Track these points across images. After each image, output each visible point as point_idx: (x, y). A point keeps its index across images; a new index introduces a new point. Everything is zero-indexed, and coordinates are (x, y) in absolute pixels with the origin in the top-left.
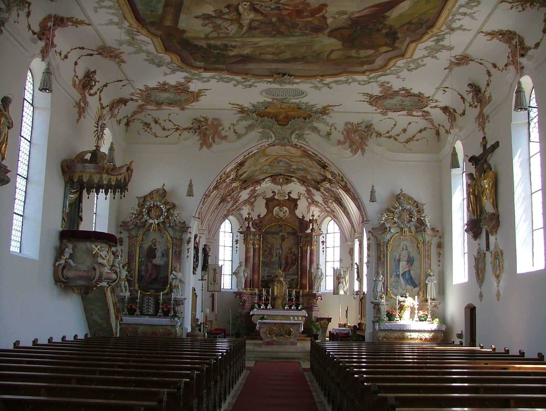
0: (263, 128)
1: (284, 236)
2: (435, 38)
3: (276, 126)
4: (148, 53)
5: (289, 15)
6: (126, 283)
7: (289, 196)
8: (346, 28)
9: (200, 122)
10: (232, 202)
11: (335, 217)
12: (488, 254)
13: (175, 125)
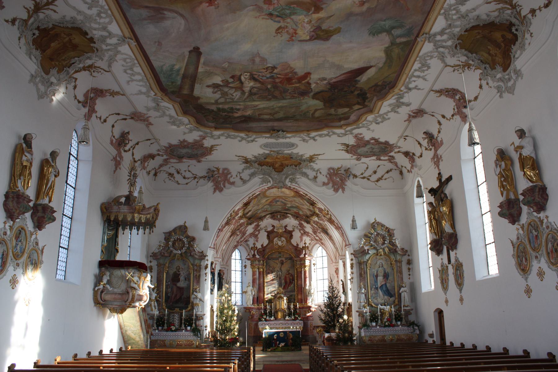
0: (263, 175)
1: (283, 261)
2: (397, 96)
3: (274, 173)
4: (171, 117)
5: (281, 82)
6: (156, 302)
7: (286, 229)
8: (326, 91)
9: (214, 171)
10: (240, 235)
11: (322, 243)
12: (450, 267)
13: (193, 174)
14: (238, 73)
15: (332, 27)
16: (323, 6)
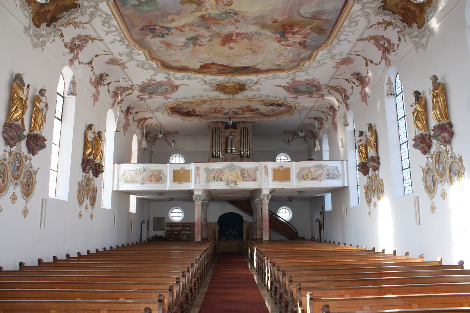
15: (188, 5)
16: (199, 19)
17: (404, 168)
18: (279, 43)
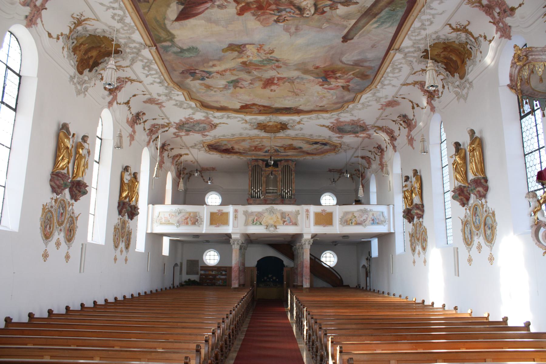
5: (270, 5)
14: (316, 17)
15: (230, 53)
16: (241, 64)
17: (447, 217)
18: (321, 87)
